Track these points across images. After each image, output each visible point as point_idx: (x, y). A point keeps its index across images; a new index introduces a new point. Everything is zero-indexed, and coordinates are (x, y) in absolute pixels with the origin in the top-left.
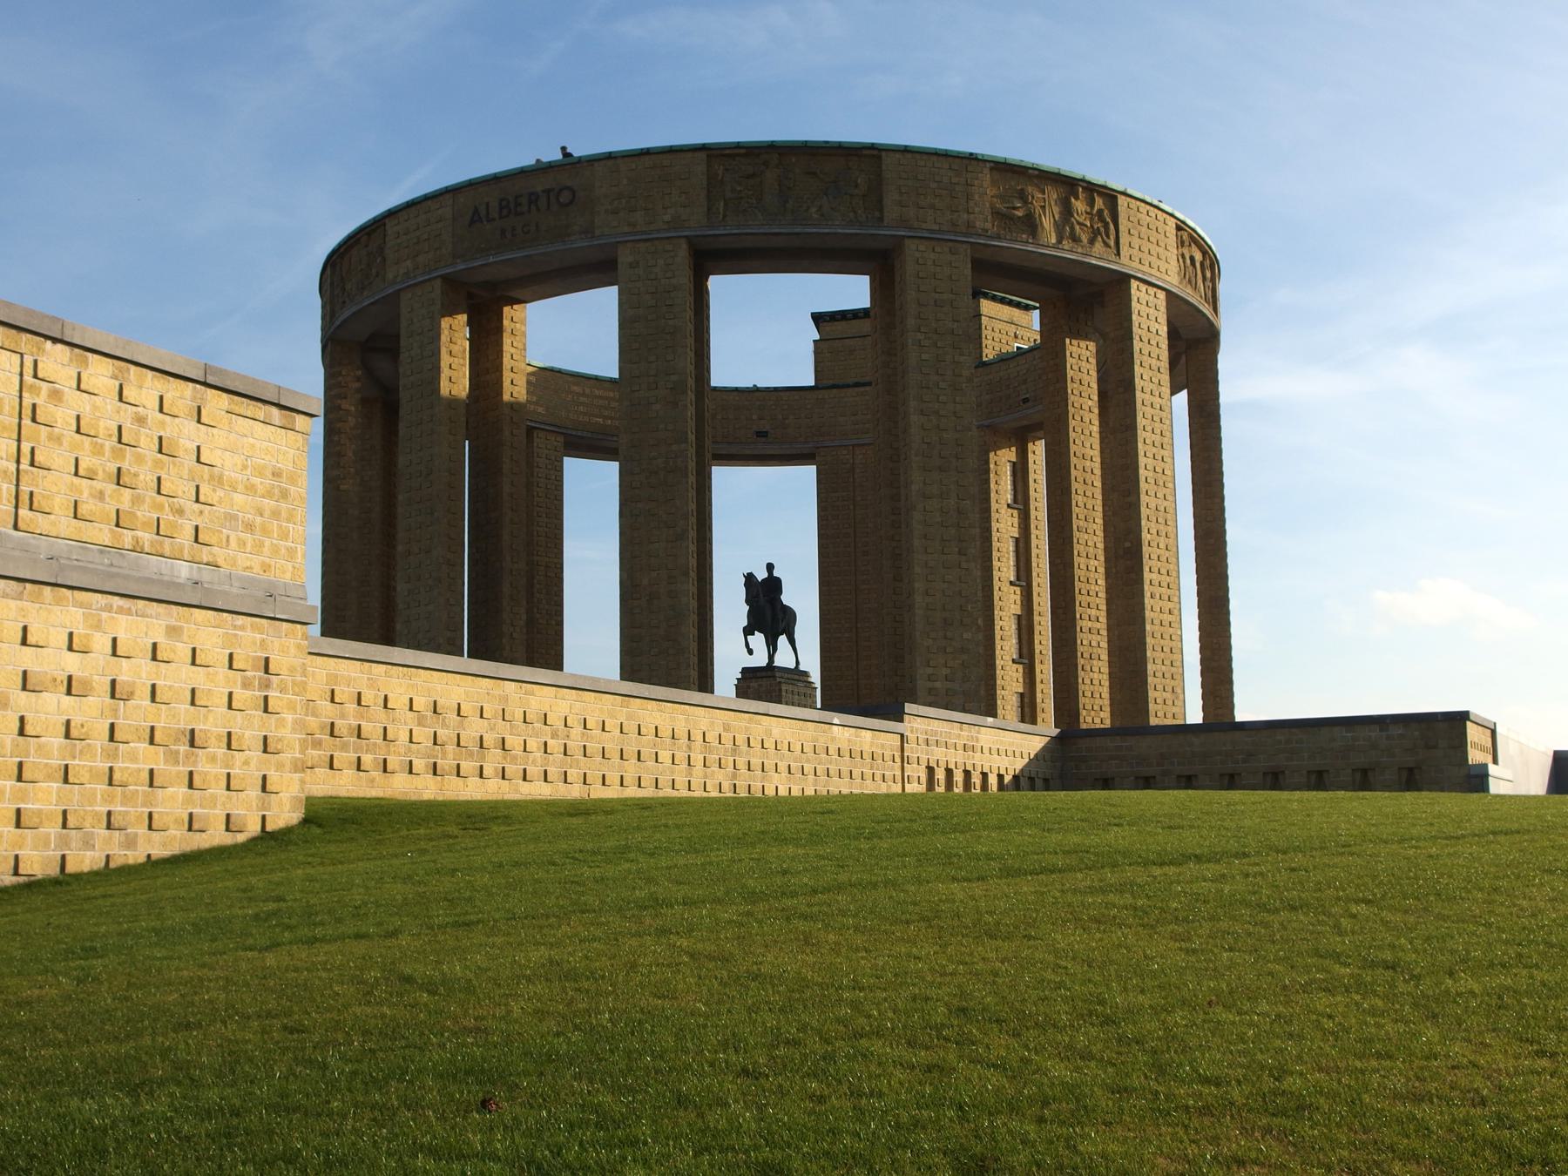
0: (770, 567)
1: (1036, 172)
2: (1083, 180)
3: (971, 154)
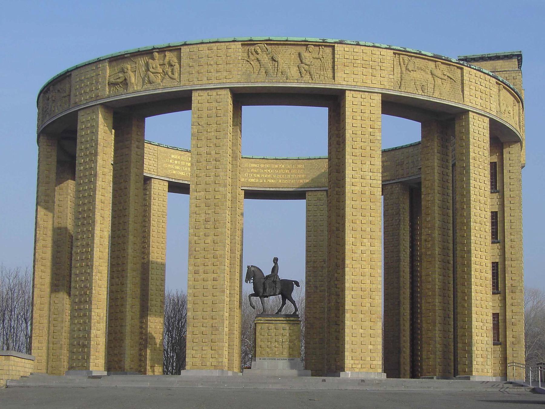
0: (276, 260)
1: (129, 55)
2: (154, 49)
3: (98, 59)
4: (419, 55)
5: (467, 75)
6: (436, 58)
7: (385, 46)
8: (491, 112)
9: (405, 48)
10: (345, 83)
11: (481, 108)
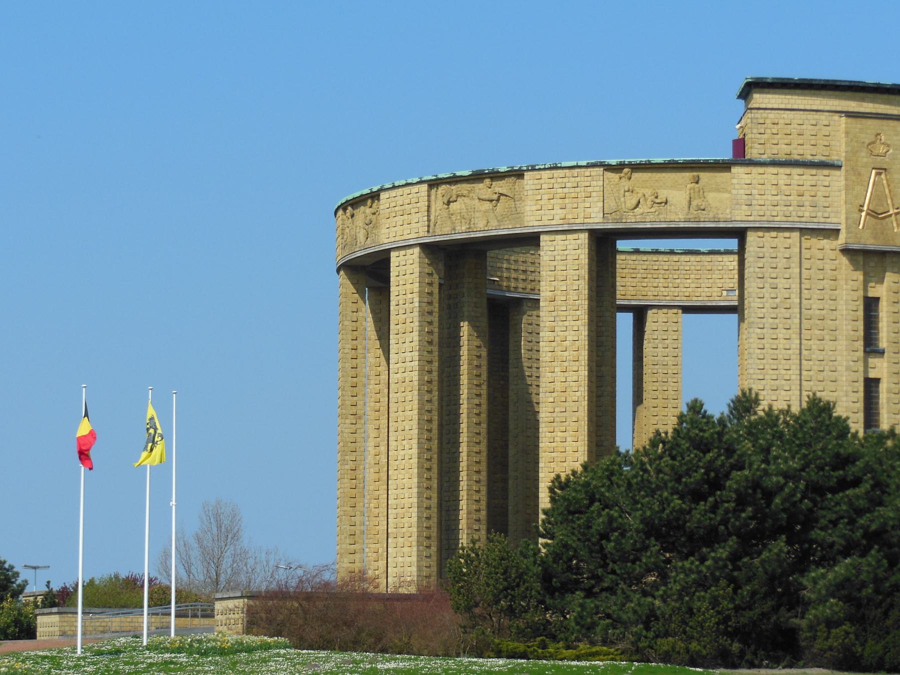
4: (454, 180)
5: (531, 182)
6: (477, 177)
7: (416, 180)
8: (586, 221)
9: (437, 176)
10: (386, 241)
11: (561, 222)
